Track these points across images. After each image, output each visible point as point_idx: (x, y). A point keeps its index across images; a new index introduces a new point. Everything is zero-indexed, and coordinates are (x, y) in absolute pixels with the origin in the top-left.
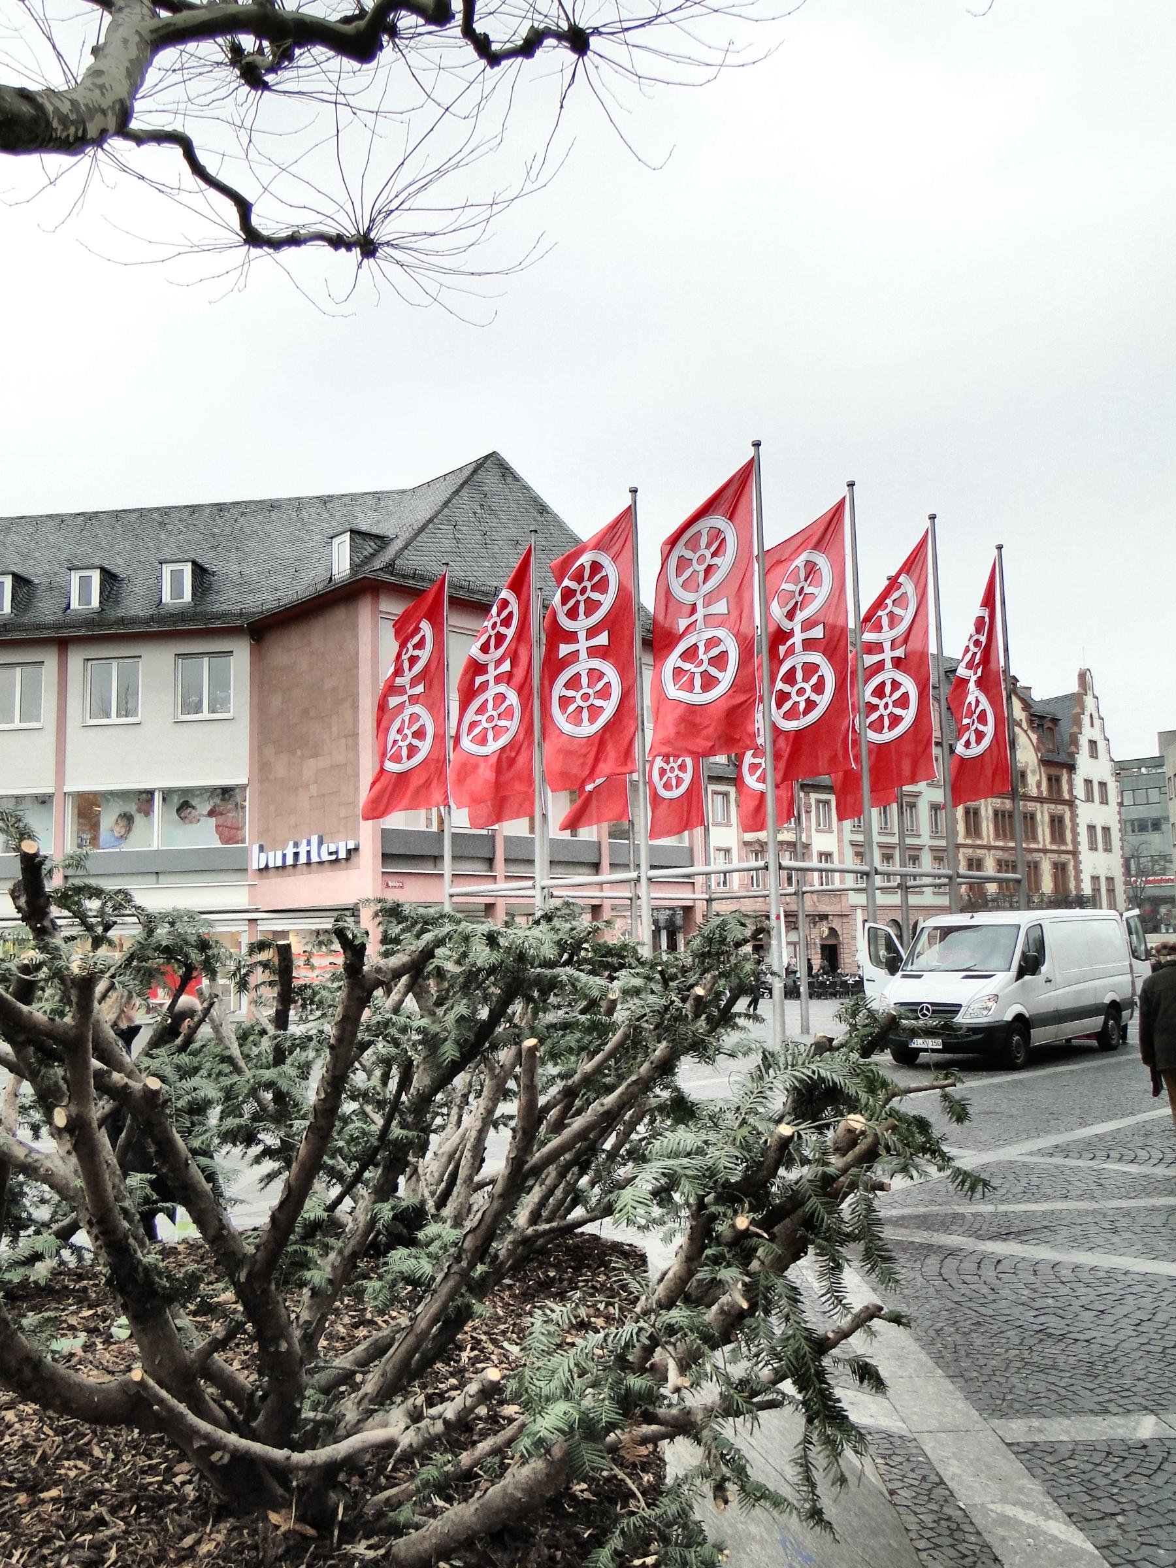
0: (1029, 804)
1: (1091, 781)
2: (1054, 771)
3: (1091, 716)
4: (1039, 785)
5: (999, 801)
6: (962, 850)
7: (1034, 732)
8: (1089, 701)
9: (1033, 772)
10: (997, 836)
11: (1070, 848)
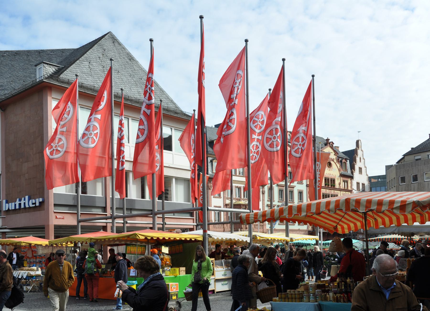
0: (336, 191)
1: (359, 183)
2: (345, 179)
3: (360, 158)
4: (340, 184)
7: (338, 163)
8: (359, 152)
9: (338, 179)
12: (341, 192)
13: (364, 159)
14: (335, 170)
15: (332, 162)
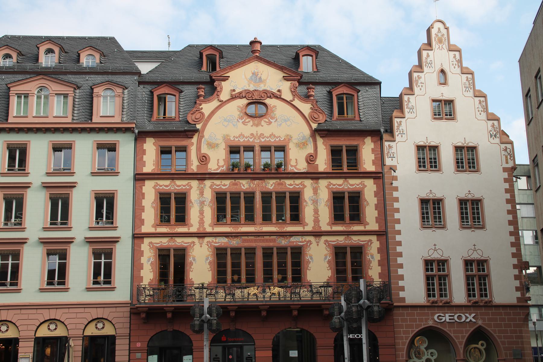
0: (288, 182)
2: (344, 142)
4: (311, 159)
5: (227, 182)
6: (147, 241)
11: (373, 226)
12: (317, 183)
13: (466, 71)
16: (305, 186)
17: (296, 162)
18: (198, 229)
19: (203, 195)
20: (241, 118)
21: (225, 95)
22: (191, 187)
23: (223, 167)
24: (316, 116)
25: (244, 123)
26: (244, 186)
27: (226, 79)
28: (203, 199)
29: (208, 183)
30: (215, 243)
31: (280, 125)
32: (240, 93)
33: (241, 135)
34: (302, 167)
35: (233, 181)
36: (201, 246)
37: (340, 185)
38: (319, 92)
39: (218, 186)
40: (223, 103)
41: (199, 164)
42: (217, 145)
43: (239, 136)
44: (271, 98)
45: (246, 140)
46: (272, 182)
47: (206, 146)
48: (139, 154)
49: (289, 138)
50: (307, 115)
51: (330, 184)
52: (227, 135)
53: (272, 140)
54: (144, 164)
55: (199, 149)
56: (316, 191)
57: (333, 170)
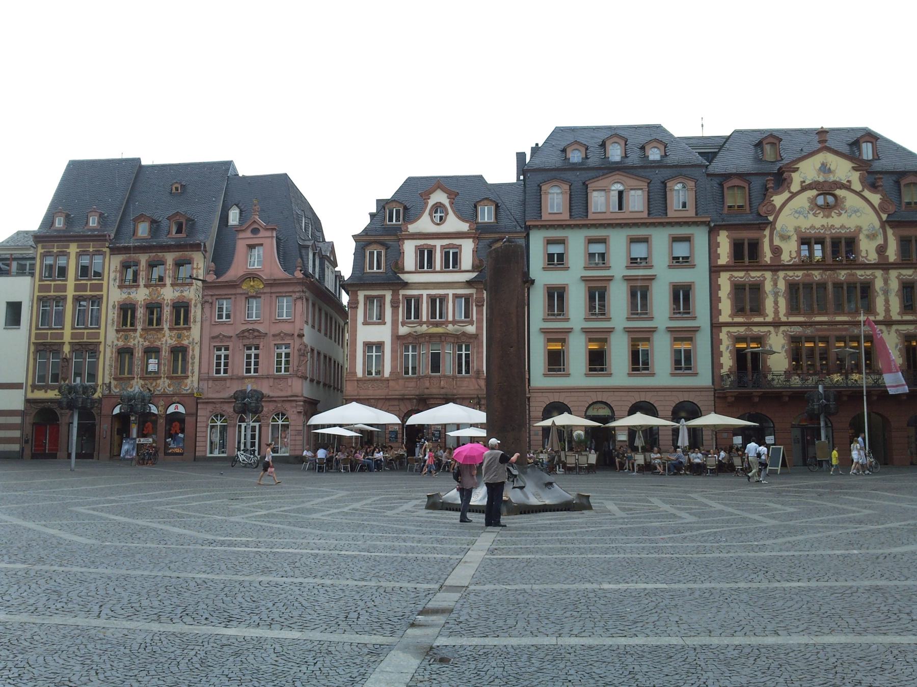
0: (859, 272)
4: (881, 250)
6: (725, 330)
10: (793, 308)
12: (887, 274)
14: (856, 211)
15: (839, 192)
16: (876, 277)
17: (867, 253)
18: (773, 319)
19: (777, 286)
20: (812, 209)
21: (795, 187)
22: (765, 279)
23: (795, 258)
24: (886, 207)
25: (815, 215)
26: (816, 277)
27: (797, 169)
28: (777, 290)
29: (781, 274)
30: (790, 332)
31: (850, 216)
32: (810, 184)
33: (813, 227)
34: (873, 257)
35: (805, 272)
36: (777, 335)
37: (910, 276)
38: (887, 182)
39: (791, 277)
40: (794, 195)
41: (772, 256)
42: (789, 237)
43: (810, 228)
44: (841, 189)
45: (817, 231)
46: (843, 272)
47: (778, 239)
48: (713, 247)
49: (859, 229)
50: (877, 206)
51: (900, 274)
52: (799, 227)
53: (843, 232)
54: (718, 256)
55: (771, 240)
56: (886, 281)
57: (902, 260)
